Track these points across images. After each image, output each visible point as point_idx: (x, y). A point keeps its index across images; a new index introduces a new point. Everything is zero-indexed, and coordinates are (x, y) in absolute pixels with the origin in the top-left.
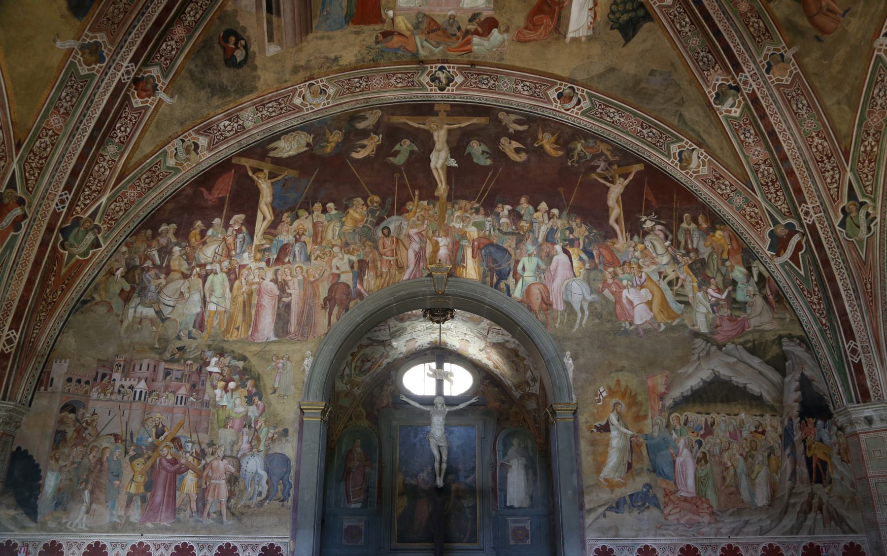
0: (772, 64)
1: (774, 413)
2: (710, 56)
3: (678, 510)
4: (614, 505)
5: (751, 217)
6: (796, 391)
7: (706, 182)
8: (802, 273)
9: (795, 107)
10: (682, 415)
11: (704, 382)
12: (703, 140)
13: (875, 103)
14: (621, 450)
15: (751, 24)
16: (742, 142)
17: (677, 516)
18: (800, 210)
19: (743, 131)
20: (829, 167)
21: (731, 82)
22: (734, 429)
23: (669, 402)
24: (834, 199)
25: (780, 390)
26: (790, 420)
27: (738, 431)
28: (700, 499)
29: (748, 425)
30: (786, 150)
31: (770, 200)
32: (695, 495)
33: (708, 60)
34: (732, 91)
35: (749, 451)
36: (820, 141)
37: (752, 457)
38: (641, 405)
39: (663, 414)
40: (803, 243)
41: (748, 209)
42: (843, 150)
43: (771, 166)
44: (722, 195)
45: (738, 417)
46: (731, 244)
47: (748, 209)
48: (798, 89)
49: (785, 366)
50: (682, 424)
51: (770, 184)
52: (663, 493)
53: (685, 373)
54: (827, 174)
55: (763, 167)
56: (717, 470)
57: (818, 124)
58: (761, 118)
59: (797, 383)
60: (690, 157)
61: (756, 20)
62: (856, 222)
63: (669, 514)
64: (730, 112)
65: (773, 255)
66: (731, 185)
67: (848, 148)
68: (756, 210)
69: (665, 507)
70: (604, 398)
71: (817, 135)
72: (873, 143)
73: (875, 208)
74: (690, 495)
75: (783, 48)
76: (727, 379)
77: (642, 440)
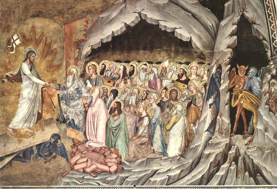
1: (202, 61)
3: (85, 160)
4: (21, 155)
6: (231, 35)
10: (98, 63)
11: (128, 27)
14: (33, 101)
17: (84, 165)
22: (155, 78)
23: (86, 50)
25: (214, 35)
26: (220, 67)
27: (158, 80)
28: (109, 149)
29: (170, 74)
32: (104, 145)
35: (168, 101)
37: (171, 107)
38: (56, 54)
39: (79, 62)
45: (161, 66)
49: (224, 7)
50: (99, 74)
52: (71, 143)
53: (107, 17)
56: (130, 120)
59: (235, 27)
63: (76, 164)
69: (72, 157)
70: (17, 46)
74: (98, 146)
76: (154, 23)
77: (54, 90)
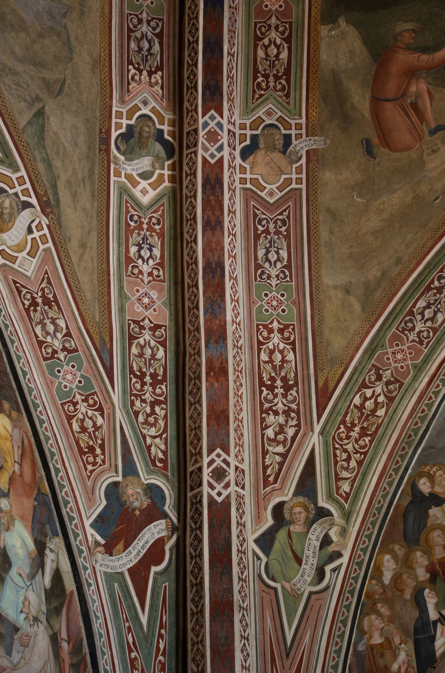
0: (262, 145)
2: (156, 47)
5: (84, 429)
7: (20, 292)
8: (144, 620)
9: (261, 253)
12: (58, 200)
13: (410, 325)
15: (266, 41)
16: (129, 260)
18: (206, 460)
19: (139, 239)
20: (280, 405)
21: (166, 128)
24: (266, 477)
30: (229, 318)
31: (136, 414)
33: (149, 50)
34: (158, 147)
36: (282, 346)
40: (167, 547)
41: (82, 407)
42: (321, 384)
43: (163, 343)
44: (41, 343)
46: (21, 465)
47: (82, 407)
48: (284, 222)
51: (148, 379)
54: (271, 419)
55: (147, 335)
57: (290, 310)
58: (207, 225)
60: (12, 217)
61: (278, 41)
62: (297, 547)
64: (135, 184)
65: (97, 544)
66: (68, 334)
67: (331, 386)
68: (100, 421)
71: (281, 331)
72: (381, 399)
73: (344, 532)
75: (298, 127)
